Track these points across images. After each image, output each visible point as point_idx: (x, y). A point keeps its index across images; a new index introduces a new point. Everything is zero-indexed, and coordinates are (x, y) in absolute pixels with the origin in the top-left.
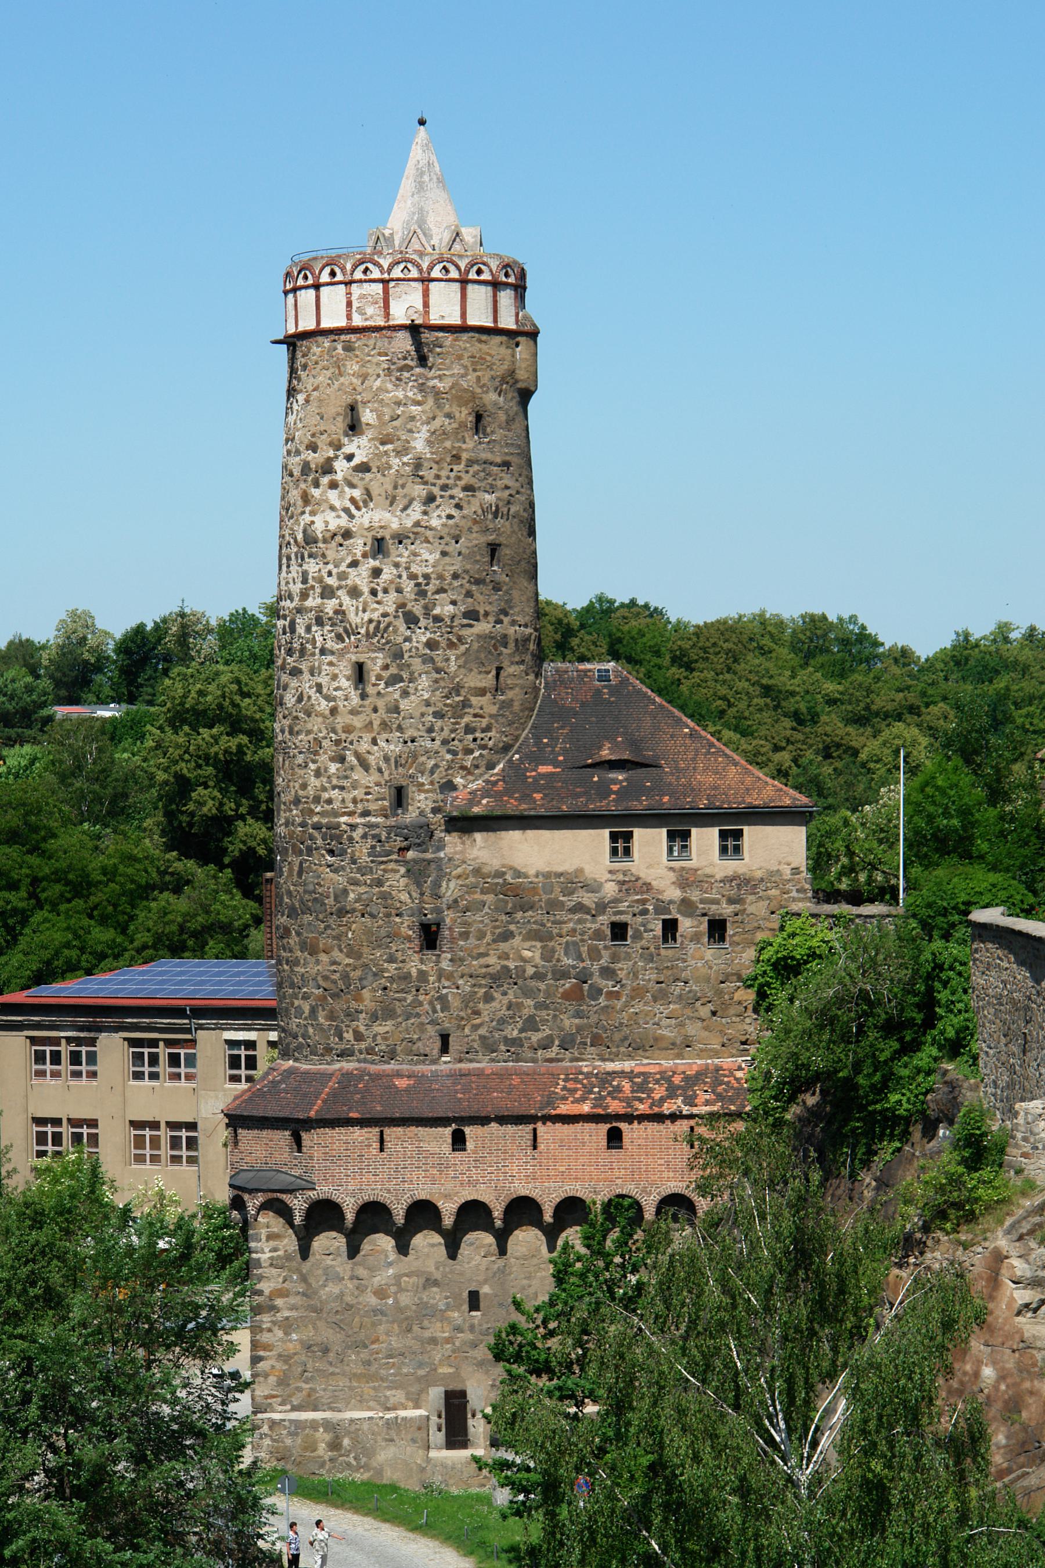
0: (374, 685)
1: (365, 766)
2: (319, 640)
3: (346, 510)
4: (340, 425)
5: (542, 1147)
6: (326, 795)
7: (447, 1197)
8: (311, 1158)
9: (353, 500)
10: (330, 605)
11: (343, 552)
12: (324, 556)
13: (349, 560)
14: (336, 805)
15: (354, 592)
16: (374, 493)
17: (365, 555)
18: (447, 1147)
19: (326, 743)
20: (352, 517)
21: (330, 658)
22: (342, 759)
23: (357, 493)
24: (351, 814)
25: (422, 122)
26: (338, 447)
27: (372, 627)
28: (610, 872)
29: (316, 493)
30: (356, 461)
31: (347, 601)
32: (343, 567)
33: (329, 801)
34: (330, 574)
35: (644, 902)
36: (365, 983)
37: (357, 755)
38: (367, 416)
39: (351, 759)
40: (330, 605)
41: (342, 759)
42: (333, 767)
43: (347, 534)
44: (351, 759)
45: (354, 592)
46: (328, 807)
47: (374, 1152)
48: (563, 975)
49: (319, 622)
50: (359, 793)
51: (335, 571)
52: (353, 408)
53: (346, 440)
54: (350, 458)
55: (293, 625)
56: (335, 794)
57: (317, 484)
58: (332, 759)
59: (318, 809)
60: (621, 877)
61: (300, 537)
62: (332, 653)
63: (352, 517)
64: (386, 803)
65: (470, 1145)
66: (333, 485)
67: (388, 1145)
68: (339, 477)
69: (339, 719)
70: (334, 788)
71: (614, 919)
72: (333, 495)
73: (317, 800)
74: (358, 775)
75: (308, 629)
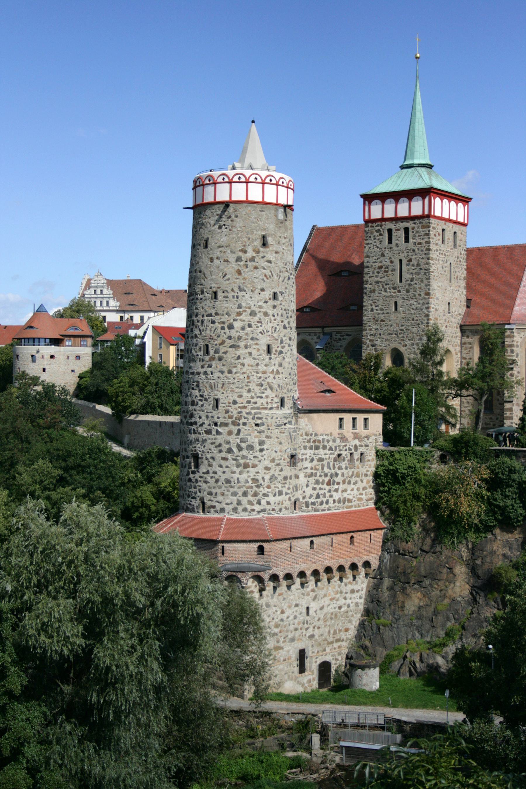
1: (271, 388)
3: (263, 280)
4: (258, 243)
5: (334, 546)
6: (253, 401)
7: (309, 569)
8: (270, 556)
9: (266, 276)
10: (256, 319)
14: (258, 405)
17: (270, 299)
18: (308, 548)
26: (258, 252)
27: (273, 329)
28: (339, 434)
33: (255, 403)
35: (346, 446)
37: (268, 383)
38: (270, 240)
40: (256, 319)
45: (266, 314)
47: (289, 552)
48: (326, 475)
53: (262, 249)
55: (231, 327)
60: (341, 436)
64: (279, 404)
65: (315, 547)
67: (293, 549)
69: (259, 367)
70: (258, 397)
71: (339, 452)
73: (249, 402)
74: (268, 392)
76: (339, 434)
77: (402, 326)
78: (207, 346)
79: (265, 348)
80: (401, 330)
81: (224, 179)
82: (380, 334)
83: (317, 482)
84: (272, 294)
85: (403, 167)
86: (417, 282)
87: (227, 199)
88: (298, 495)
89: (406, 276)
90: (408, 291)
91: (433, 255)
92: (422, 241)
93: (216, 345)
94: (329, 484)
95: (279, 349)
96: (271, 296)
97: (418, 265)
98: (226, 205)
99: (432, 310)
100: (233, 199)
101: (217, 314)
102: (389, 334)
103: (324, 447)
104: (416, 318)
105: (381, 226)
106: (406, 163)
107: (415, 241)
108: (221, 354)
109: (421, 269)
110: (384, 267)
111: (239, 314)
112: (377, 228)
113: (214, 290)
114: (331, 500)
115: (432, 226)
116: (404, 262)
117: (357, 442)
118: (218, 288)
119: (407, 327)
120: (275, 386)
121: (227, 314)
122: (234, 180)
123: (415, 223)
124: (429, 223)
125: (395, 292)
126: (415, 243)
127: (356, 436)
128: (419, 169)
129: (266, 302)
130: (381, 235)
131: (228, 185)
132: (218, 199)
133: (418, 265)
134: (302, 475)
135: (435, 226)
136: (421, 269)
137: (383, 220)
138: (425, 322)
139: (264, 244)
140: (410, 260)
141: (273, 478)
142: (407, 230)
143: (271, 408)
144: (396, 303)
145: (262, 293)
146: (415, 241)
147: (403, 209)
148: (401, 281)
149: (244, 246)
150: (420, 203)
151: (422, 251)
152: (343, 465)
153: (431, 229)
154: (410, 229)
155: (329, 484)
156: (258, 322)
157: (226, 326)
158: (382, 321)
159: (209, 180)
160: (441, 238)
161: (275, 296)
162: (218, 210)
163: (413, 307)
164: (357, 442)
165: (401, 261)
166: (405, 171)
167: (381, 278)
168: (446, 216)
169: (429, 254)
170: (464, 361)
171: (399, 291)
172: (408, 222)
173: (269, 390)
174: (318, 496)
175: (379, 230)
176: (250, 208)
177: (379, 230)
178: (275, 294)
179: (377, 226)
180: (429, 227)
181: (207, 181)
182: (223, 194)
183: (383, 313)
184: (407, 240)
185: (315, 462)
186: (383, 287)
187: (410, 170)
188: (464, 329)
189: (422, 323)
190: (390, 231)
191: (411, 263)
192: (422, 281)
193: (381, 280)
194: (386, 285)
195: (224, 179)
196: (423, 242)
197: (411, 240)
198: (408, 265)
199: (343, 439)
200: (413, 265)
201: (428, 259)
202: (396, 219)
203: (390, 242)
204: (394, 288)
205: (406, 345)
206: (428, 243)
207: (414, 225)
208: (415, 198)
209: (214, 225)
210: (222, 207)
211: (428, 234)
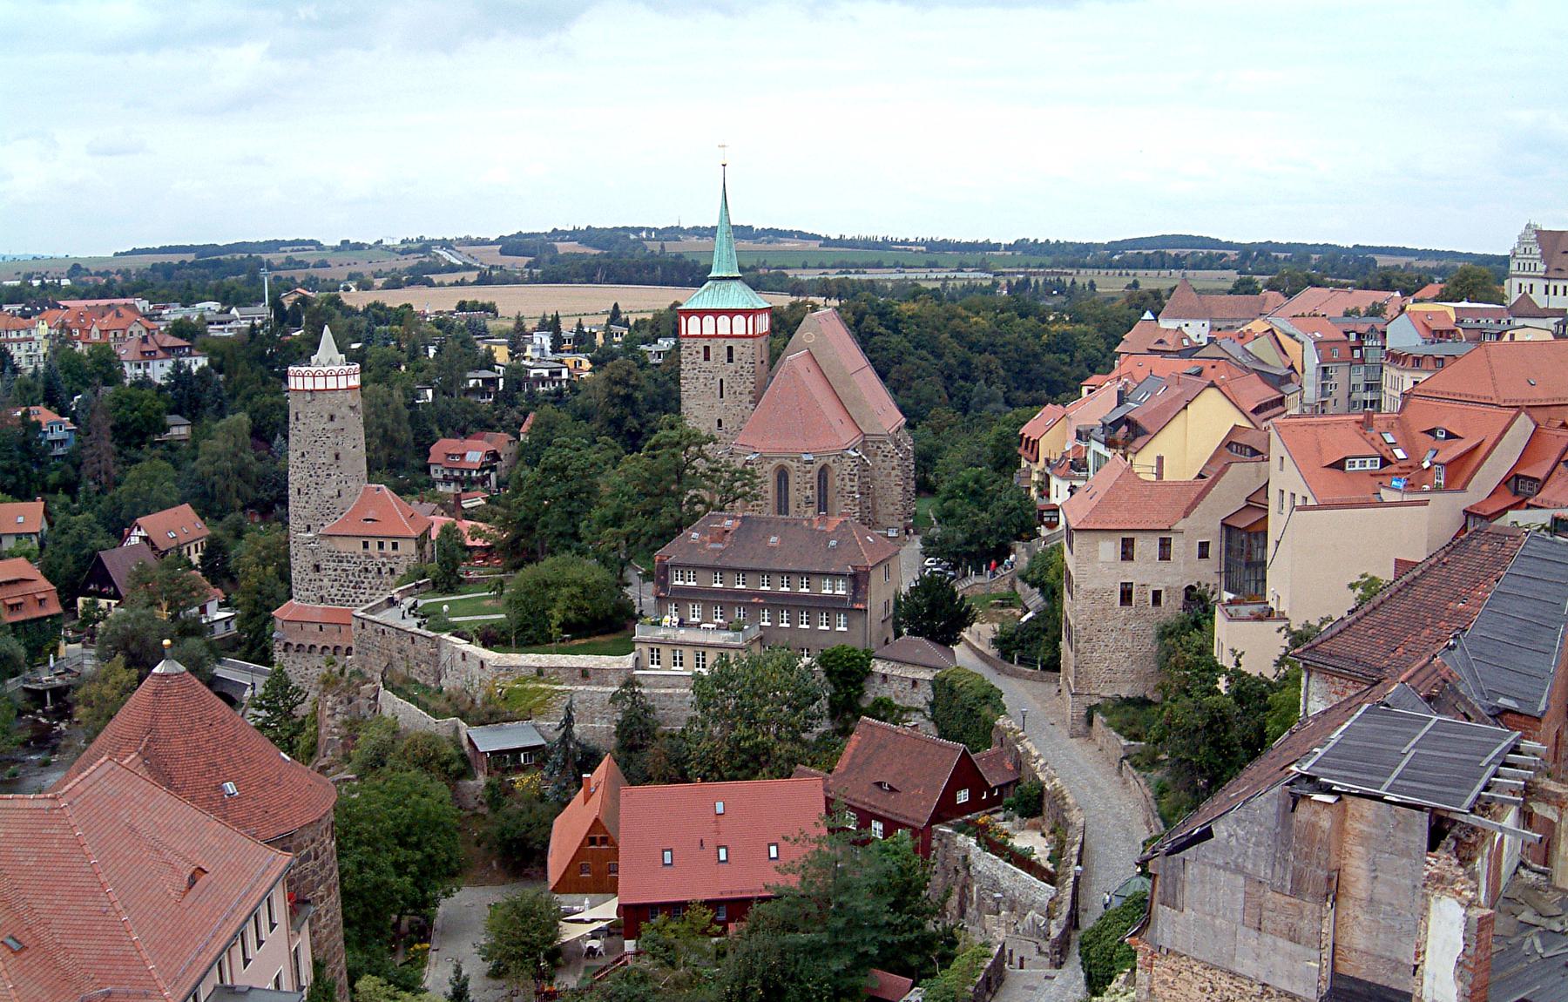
83: (342, 586)
88: (323, 592)
94: (354, 587)
103: (349, 562)
114: (357, 600)
117: (385, 560)
127: (383, 555)
134: (326, 580)
141: (302, 579)
152: (370, 575)
155: (354, 587)
161: (303, 455)
164: (385, 560)
174: (343, 595)
185: (339, 572)
199: (368, 556)
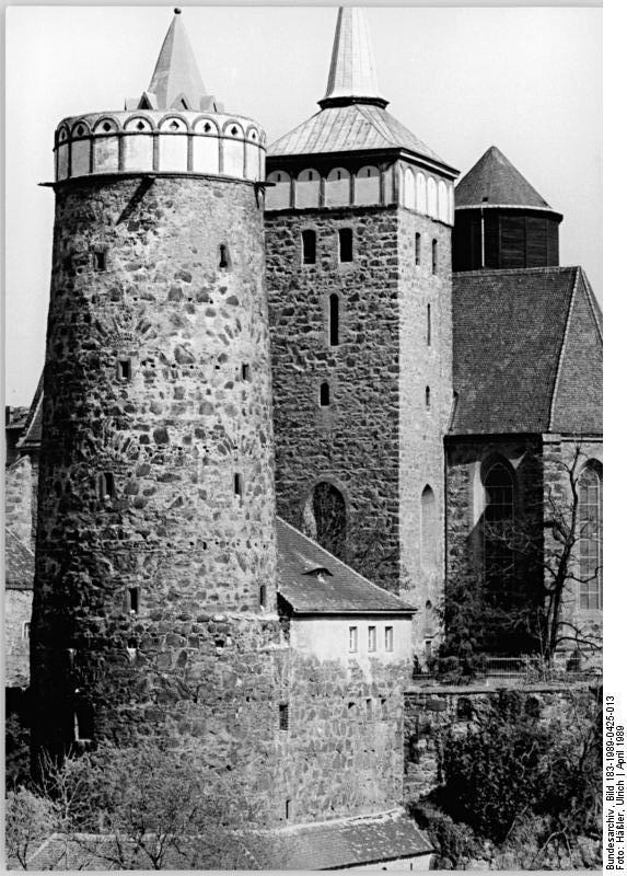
0: (248, 494)
2: (202, 453)
3: (221, 336)
6: (210, 592)
9: (227, 329)
10: (210, 422)
11: (220, 374)
12: (201, 375)
13: (226, 382)
15: (230, 410)
16: (242, 324)
17: (237, 380)
19: (211, 545)
20: (227, 343)
21: (213, 468)
22: (226, 560)
23: (232, 324)
24: (234, 609)
25: (177, 12)
26: (213, 280)
28: (350, 661)
29: (192, 318)
30: (228, 294)
31: (225, 418)
32: (221, 387)
33: (215, 597)
34: (209, 392)
36: (249, 758)
38: (233, 255)
39: (234, 559)
41: (226, 560)
42: (219, 566)
43: (223, 358)
44: (234, 559)
45: (230, 410)
46: (214, 603)
49: (200, 434)
50: (240, 591)
51: (213, 390)
52: (223, 248)
53: (219, 275)
54: (223, 290)
55: (162, 437)
56: (219, 591)
57: (192, 310)
58: (217, 560)
59: (204, 604)
60: (352, 665)
61: (170, 357)
62: (215, 463)
63: (227, 343)
66: (210, 313)
68: (215, 306)
70: (219, 585)
72: (209, 320)
75: (187, 440)
76: (350, 661)
77: (338, 436)
78: (109, 477)
79: (231, 481)
80: (336, 445)
81: (141, 126)
82: (291, 454)
84: (240, 367)
85: (326, 104)
86: (370, 344)
87: (147, 168)
89: (345, 330)
90: (351, 363)
91: (402, 287)
92: (380, 259)
93: (130, 475)
95: (254, 485)
96: (240, 372)
97: (373, 308)
98: (147, 181)
99: (401, 403)
100: (162, 169)
101: (130, 409)
102: (312, 454)
104: (369, 421)
105: (289, 225)
106: (334, 95)
107: (363, 257)
108: (141, 495)
109: (379, 316)
110: (296, 312)
111: (179, 409)
112: (281, 229)
113: (123, 357)
115: (400, 226)
116: (343, 301)
118: (131, 354)
119: (350, 440)
120: (248, 561)
121: (152, 410)
122: (163, 129)
123: (363, 222)
124: (396, 220)
125: (323, 365)
126: (365, 261)
128: (363, 108)
129: (230, 386)
130: (289, 243)
131: (149, 139)
132: (130, 167)
133: (373, 308)
135: (405, 227)
136: (379, 316)
137: (292, 212)
138: (390, 428)
139: (224, 264)
140: (355, 298)
142: (346, 235)
143: (245, 608)
144: (325, 388)
145: (223, 366)
146: (363, 257)
147: (337, 191)
148: (335, 341)
149: (185, 266)
150: (375, 180)
151: (382, 278)
153: (398, 233)
154: (355, 233)
156: (216, 427)
157: (150, 434)
158: (295, 425)
159: (107, 127)
160: (413, 251)
162: (131, 188)
163: (363, 396)
165: (334, 299)
166: (334, 111)
167: (290, 334)
168: (421, 210)
169: (396, 286)
170: (453, 510)
171: (332, 363)
172: (349, 217)
173: (239, 569)
175: (284, 232)
176: (194, 187)
177: (284, 232)
178: (245, 367)
179: (278, 225)
180: (395, 229)
181: (100, 130)
182: (138, 157)
183: (297, 410)
184: (347, 256)
186: (295, 352)
187: (345, 110)
188: (457, 448)
189: (383, 430)
190: (310, 237)
191: (357, 304)
192: (382, 342)
193: (290, 339)
194: (303, 348)
195: (141, 126)
196: (383, 259)
197: (356, 256)
198: (349, 308)
200: (362, 309)
201: (394, 296)
202: (321, 213)
203: (310, 258)
204: (320, 357)
205: (348, 477)
206: (394, 262)
207: (362, 225)
208: (364, 170)
209: (118, 223)
210: (136, 184)
211: (394, 245)
